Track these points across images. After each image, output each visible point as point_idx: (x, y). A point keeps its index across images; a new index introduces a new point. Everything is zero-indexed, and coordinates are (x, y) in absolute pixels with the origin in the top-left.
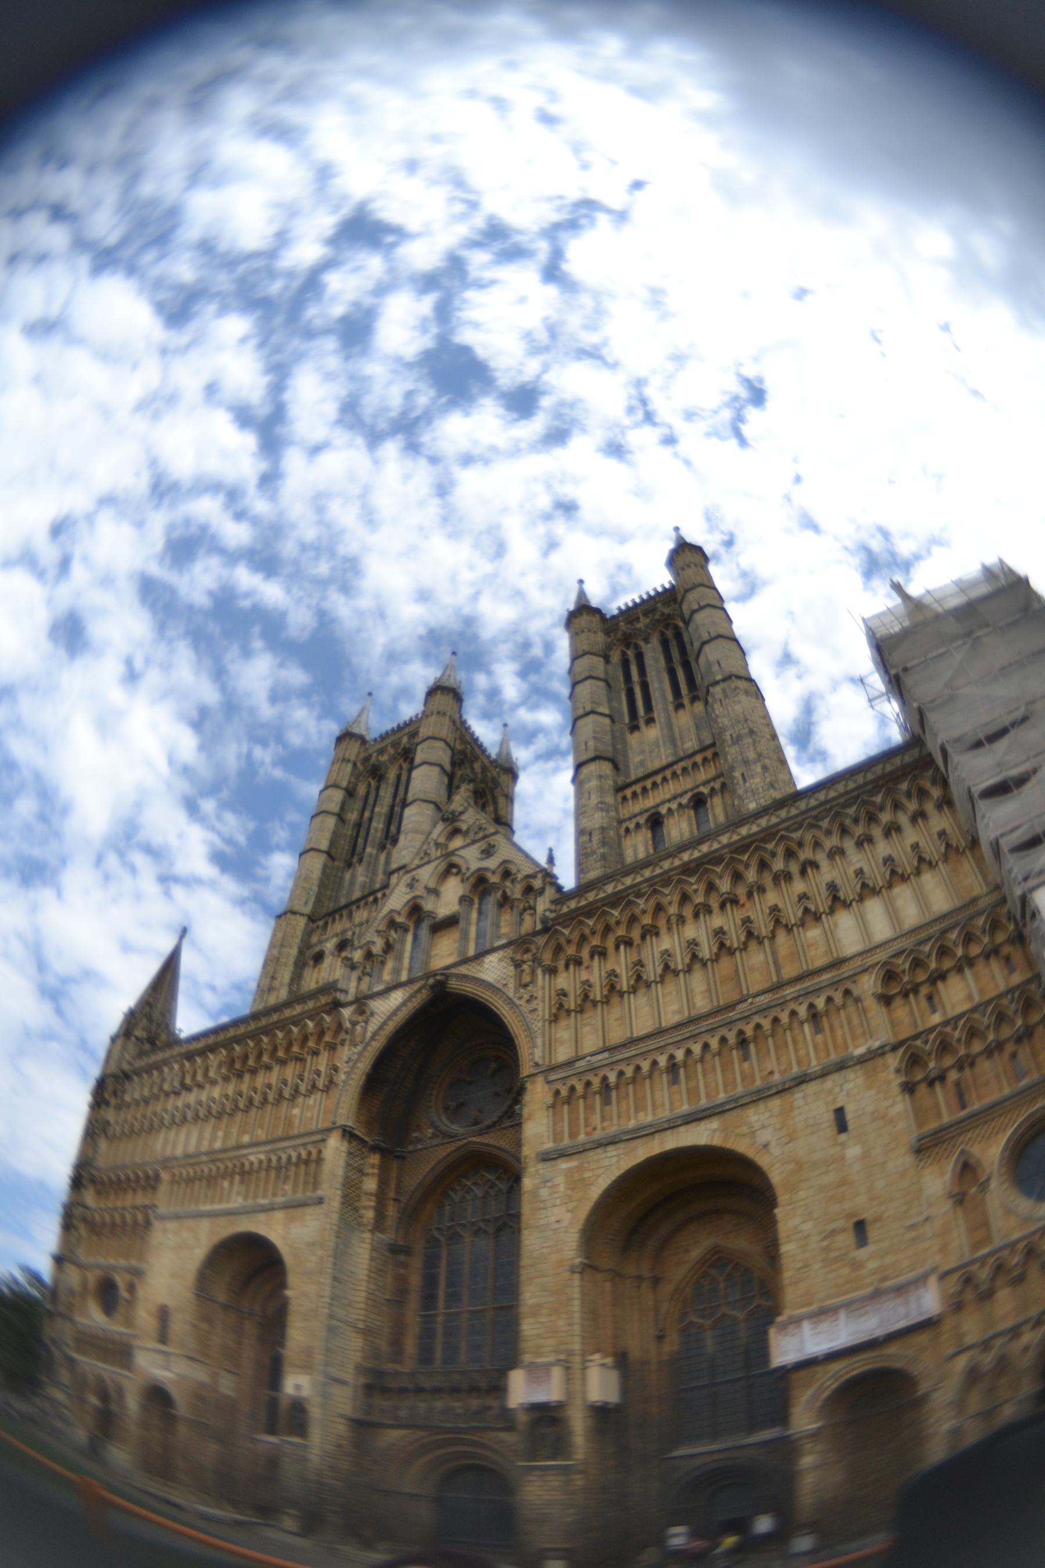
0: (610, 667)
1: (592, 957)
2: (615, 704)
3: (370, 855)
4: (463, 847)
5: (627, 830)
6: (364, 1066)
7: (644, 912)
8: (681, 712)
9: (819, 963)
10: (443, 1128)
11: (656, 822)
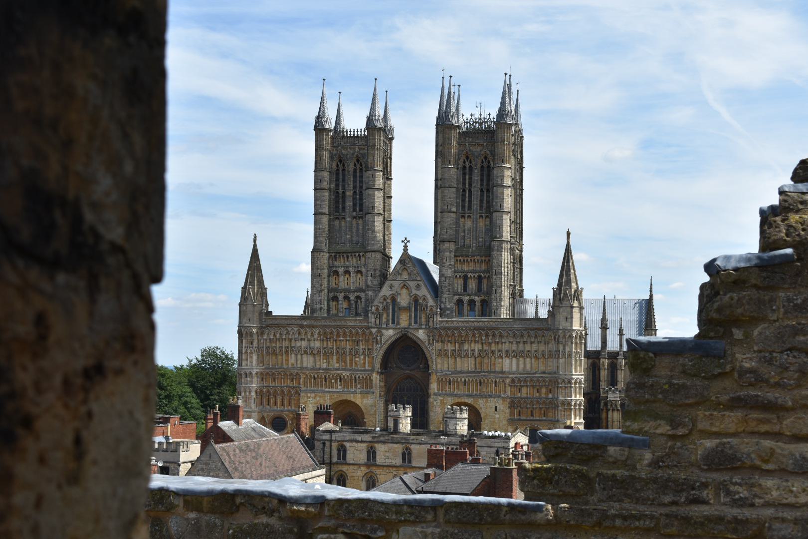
2: (458, 201)
3: (349, 222)
6: (382, 352)
8: (481, 219)
9: (499, 370)
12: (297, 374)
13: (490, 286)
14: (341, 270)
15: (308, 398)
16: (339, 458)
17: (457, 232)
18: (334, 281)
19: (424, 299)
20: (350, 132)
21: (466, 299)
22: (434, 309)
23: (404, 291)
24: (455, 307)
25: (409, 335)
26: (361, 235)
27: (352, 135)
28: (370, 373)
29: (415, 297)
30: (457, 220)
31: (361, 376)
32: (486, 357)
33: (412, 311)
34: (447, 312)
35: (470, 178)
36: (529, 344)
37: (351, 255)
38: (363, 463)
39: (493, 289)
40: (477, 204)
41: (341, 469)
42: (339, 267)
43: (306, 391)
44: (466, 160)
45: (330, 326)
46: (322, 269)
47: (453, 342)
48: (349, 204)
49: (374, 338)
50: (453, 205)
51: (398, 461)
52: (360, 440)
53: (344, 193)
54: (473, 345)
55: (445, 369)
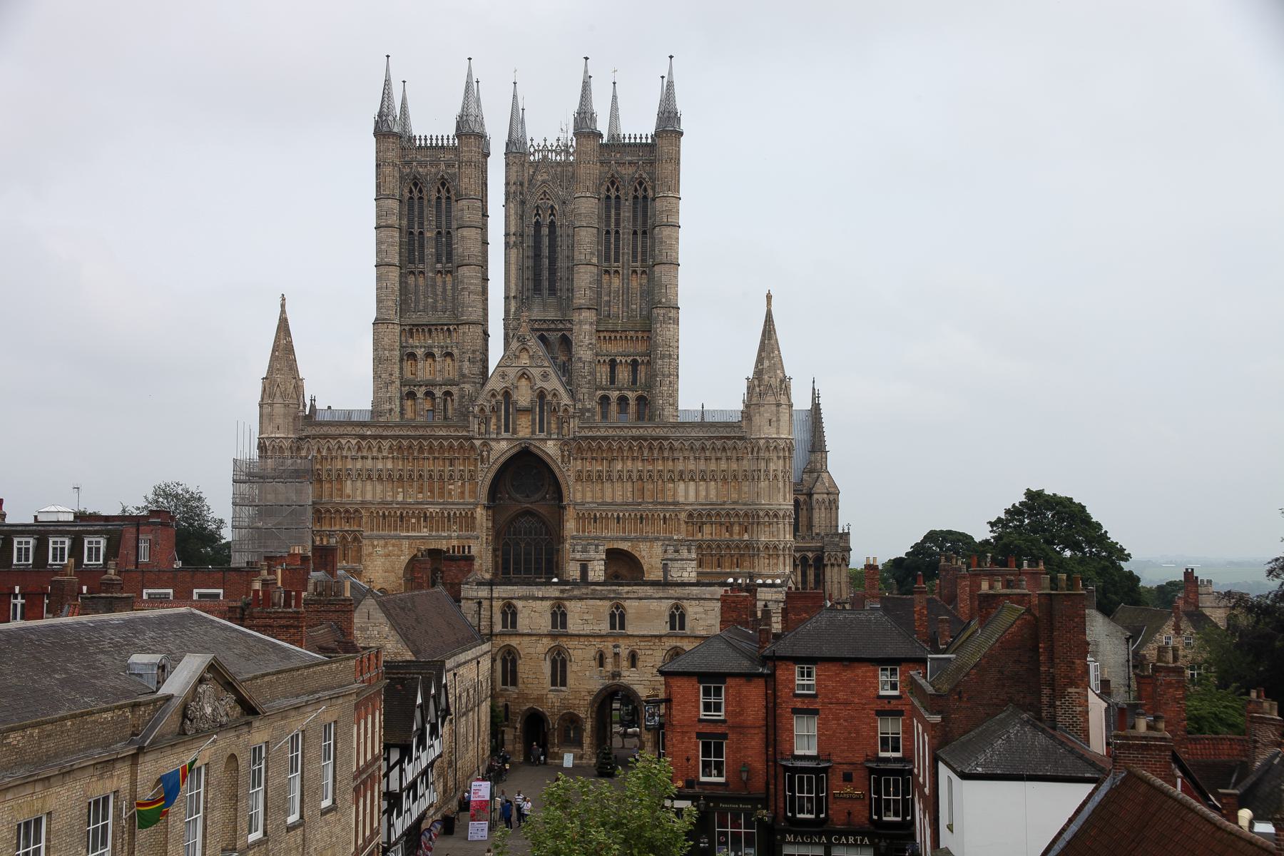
2: (600, 248)
3: (432, 278)
6: (491, 475)
7: (615, 450)
12: (356, 511)
13: (652, 376)
14: (420, 352)
15: (374, 547)
16: (505, 626)
17: (599, 295)
19: (555, 394)
20: (431, 139)
21: (614, 395)
22: (571, 410)
23: (524, 382)
24: (598, 408)
25: (532, 448)
26: (449, 298)
27: (434, 145)
28: (472, 507)
29: (541, 391)
30: (599, 275)
31: (458, 513)
32: (650, 481)
33: (535, 412)
34: (587, 414)
35: (618, 214)
36: (713, 461)
37: (436, 329)
38: (546, 632)
40: (628, 253)
41: (508, 643)
42: (416, 347)
43: (370, 538)
44: (610, 186)
45: (408, 437)
46: (392, 350)
48: (430, 250)
51: (605, 627)
52: (540, 596)
53: (421, 233)
54: (629, 463)
55: (588, 500)
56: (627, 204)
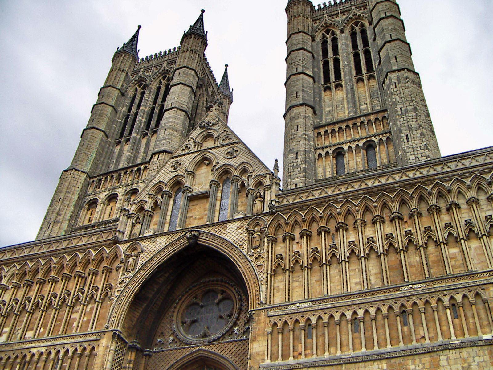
0: (314, 43)
1: (302, 237)
2: (316, 70)
3: (135, 138)
4: (214, 148)
5: (320, 155)
7: (339, 214)
8: (360, 84)
10: (180, 336)
11: (339, 154)
18: (88, 216)
19: (244, 171)
25: (204, 240)
39: (403, 135)
47: (314, 233)
49: (122, 262)
50: (309, 69)
56: (343, 35)
